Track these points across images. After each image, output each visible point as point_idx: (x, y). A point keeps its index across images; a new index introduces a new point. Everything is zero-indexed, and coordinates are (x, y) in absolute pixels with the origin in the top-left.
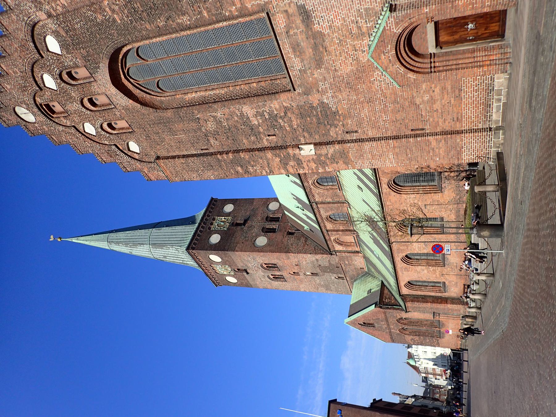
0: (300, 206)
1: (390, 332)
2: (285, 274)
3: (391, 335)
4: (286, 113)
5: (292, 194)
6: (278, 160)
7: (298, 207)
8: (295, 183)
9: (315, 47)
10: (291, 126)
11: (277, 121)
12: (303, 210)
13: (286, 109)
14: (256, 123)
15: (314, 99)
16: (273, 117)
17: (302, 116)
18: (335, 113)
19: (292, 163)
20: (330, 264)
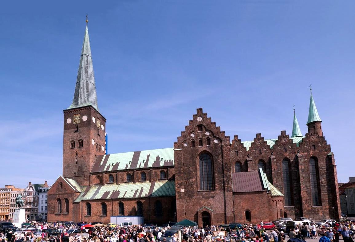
0: (114, 164)
1: (57, 195)
2: (76, 149)
3: (54, 195)
4: (192, 188)
5: (119, 162)
6: (180, 183)
7: (113, 163)
8: (127, 166)
9: (206, 197)
10: (189, 188)
11: (191, 185)
12: (112, 165)
13: (194, 188)
14: (191, 180)
15: (195, 194)
16: (192, 185)
17: (191, 191)
18: (191, 198)
19: (179, 186)
20: (84, 171)
